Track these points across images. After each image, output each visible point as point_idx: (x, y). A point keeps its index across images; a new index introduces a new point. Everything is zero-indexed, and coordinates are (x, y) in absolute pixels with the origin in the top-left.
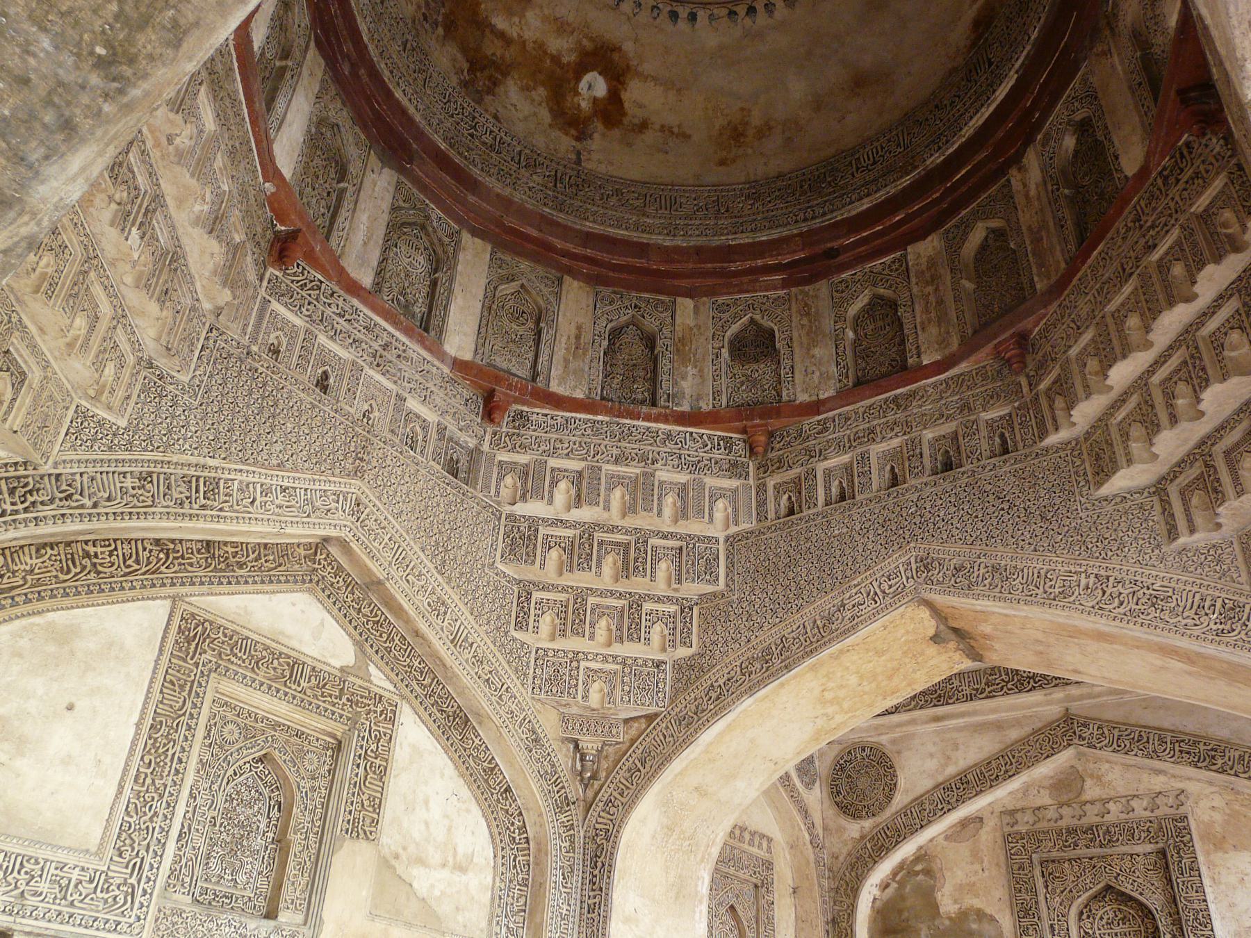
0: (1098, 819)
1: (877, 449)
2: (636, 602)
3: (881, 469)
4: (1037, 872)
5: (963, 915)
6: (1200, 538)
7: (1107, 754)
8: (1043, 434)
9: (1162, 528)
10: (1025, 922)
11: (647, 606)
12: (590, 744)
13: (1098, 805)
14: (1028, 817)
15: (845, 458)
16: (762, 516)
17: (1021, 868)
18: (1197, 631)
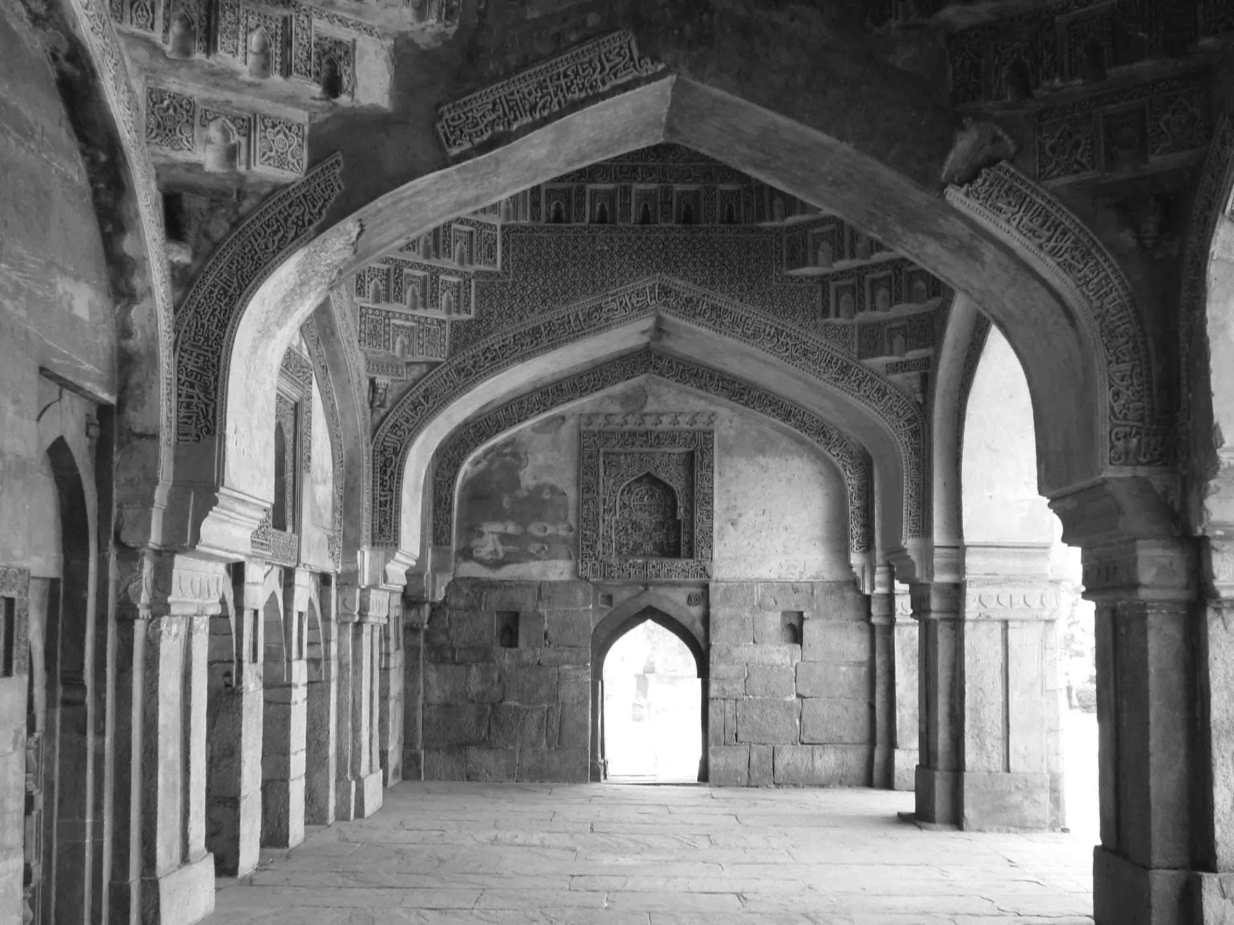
0: (653, 427)
1: (638, 187)
2: (436, 272)
3: (638, 205)
4: (601, 460)
5: (539, 489)
6: (839, 321)
7: (672, 382)
8: (761, 218)
9: (819, 307)
10: (586, 496)
11: (442, 277)
12: (382, 380)
13: (654, 418)
14: (601, 420)
15: (610, 186)
16: (535, 217)
17: (590, 457)
18: (825, 376)
